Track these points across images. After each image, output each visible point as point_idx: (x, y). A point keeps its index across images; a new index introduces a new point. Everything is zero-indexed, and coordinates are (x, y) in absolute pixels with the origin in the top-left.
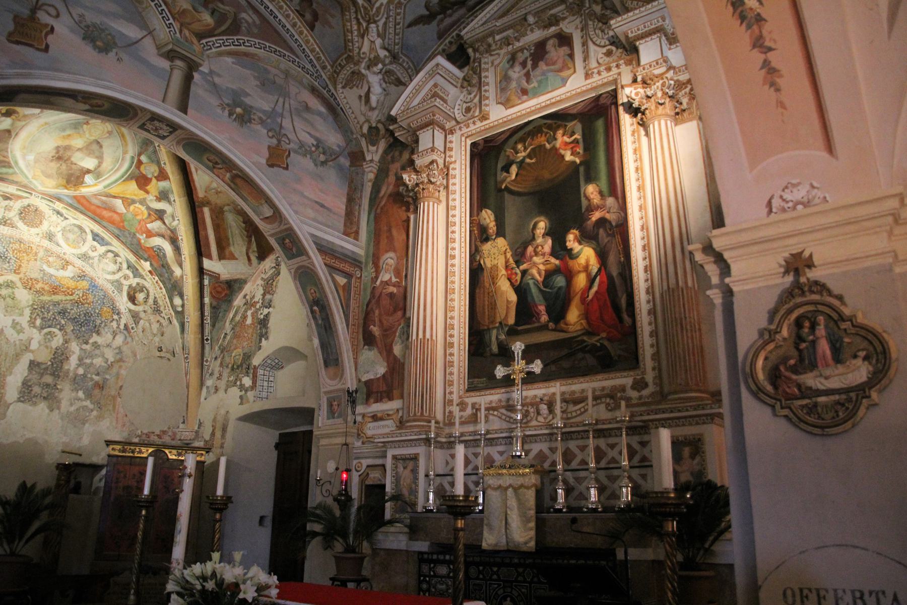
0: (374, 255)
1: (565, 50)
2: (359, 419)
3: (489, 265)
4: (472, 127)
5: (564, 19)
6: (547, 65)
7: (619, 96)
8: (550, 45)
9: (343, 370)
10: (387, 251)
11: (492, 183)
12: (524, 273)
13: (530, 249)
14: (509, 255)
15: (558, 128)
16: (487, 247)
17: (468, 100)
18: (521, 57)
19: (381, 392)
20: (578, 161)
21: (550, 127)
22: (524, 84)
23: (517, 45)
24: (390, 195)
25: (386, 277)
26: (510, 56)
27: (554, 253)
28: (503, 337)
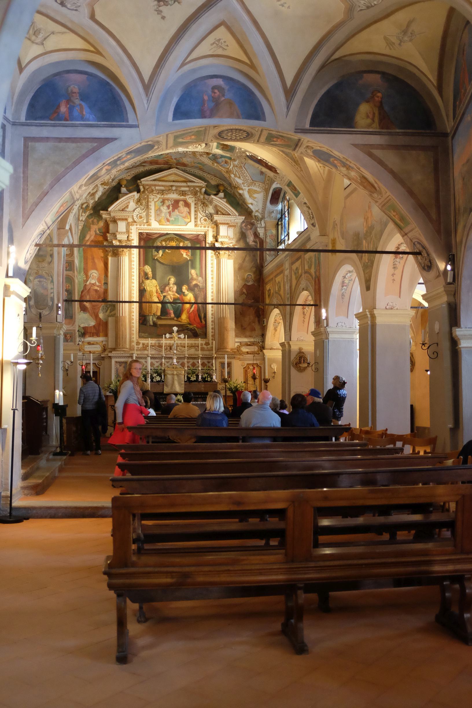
0: (84, 269)
1: (186, 209)
2: (80, 343)
3: (148, 289)
4: (142, 226)
5: (188, 195)
6: (179, 212)
7: (207, 240)
8: (181, 204)
9: (75, 322)
10: (93, 269)
11: (150, 255)
12: (164, 296)
13: (167, 288)
14: (158, 288)
15: (181, 241)
16: (147, 282)
17: (140, 212)
18: (167, 203)
19: (93, 333)
20: (189, 259)
21: (177, 240)
22: (168, 215)
23: (166, 196)
24: (92, 241)
25: (93, 282)
26: (161, 200)
27: (177, 292)
28: (155, 319)
